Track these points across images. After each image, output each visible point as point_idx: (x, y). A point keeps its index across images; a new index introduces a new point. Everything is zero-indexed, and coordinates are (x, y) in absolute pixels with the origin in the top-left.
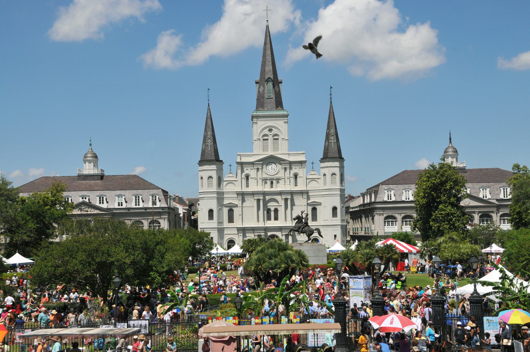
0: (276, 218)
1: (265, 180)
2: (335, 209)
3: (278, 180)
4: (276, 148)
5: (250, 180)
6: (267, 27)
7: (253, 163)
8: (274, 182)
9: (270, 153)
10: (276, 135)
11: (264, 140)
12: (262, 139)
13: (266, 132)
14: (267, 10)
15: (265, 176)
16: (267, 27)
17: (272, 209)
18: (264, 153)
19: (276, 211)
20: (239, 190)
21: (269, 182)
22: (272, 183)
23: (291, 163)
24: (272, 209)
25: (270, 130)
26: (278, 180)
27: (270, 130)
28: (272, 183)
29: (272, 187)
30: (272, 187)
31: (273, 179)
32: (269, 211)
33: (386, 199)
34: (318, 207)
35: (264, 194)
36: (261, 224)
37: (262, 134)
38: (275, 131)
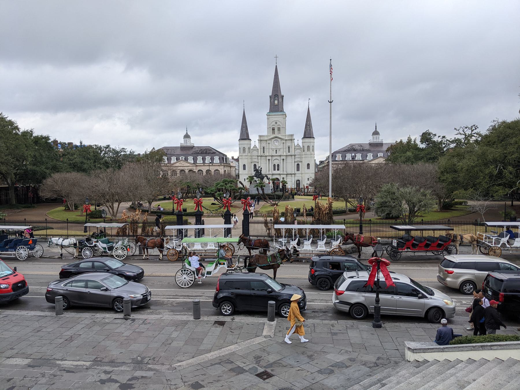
0: (278, 170)
2: (308, 165)
3: (280, 149)
7: (266, 141)
8: (278, 150)
9: (276, 135)
13: (274, 123)
15: (274, 147)
17: (276, 165)
19: (278, 165)
23: (286, 140)
24: (276, 165)
25: (276, 123)
26: (280, 149)
27: (276, 123)
33: (337, 159)
34: (300, 163)
35: (272, 156)
38: (278, 123)
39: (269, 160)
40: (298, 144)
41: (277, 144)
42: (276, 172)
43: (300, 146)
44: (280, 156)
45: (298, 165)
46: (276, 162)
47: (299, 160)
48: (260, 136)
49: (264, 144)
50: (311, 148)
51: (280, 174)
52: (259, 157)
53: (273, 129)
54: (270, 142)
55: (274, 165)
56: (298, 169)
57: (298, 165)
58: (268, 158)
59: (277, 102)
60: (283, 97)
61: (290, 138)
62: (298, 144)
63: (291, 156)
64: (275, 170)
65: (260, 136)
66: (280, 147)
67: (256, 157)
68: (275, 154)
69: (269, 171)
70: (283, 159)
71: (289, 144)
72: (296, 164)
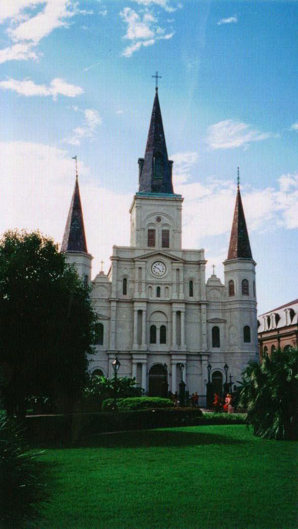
0: (163, 341)
1: (149, 285)
3: (168, 285)
4: (166, 243)
5: (130, 286)
6: (157, 95)
7: (133, 260)
10: (166, 225)
11: (149, 231)
12: (147, 231)
13: (153, 220)
14: (157, 77)
15: (150, 279)
16: (157, 95)
17: (158, 327)
18: (149, 248)
19: (163, 329)
20: (113, 296)
21: (155, 288)
22: (159, 289)
24: (158, 327)
25: (159, 220)
27: (159, 220)
28: (159, 289)
29: (158, 295)
30: (158, 295)
31: (161, 284)
32: (153, 329)
34: (221, 326)
35: (148, 302)
36: (144, 347)
37: (147, 223)
38: (165, 220)
39: (140, 312)
40: (214, 276)
41: (162, 271)
42: (158, 347)
43: (219, 280)
44: (170, 303)
45: (216, 331)
46: (159, 321)
47: (219, 316)
48: (116, 249)
49: (126, 271)
50: (250, 284)
51: (169, 354)
52: (114, 304)
53: (151, 234)
54: (142, 264)
55: (153, 329)
56: (216, 342)
57: (216, 331)
58: (138, 306)
59: (157, 172)
60: (171, 162)
61: (194, 258)
62: (214, 276)
63: (199, 304)
64: (153, 341)
65: (116, 249)
66: (168, 280)
67: (106, 305)
68: (154, 297)
69: (140, 343)
70: (179, 313)
71: (192, 273)
72: (211, 326)
